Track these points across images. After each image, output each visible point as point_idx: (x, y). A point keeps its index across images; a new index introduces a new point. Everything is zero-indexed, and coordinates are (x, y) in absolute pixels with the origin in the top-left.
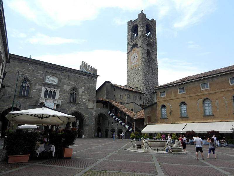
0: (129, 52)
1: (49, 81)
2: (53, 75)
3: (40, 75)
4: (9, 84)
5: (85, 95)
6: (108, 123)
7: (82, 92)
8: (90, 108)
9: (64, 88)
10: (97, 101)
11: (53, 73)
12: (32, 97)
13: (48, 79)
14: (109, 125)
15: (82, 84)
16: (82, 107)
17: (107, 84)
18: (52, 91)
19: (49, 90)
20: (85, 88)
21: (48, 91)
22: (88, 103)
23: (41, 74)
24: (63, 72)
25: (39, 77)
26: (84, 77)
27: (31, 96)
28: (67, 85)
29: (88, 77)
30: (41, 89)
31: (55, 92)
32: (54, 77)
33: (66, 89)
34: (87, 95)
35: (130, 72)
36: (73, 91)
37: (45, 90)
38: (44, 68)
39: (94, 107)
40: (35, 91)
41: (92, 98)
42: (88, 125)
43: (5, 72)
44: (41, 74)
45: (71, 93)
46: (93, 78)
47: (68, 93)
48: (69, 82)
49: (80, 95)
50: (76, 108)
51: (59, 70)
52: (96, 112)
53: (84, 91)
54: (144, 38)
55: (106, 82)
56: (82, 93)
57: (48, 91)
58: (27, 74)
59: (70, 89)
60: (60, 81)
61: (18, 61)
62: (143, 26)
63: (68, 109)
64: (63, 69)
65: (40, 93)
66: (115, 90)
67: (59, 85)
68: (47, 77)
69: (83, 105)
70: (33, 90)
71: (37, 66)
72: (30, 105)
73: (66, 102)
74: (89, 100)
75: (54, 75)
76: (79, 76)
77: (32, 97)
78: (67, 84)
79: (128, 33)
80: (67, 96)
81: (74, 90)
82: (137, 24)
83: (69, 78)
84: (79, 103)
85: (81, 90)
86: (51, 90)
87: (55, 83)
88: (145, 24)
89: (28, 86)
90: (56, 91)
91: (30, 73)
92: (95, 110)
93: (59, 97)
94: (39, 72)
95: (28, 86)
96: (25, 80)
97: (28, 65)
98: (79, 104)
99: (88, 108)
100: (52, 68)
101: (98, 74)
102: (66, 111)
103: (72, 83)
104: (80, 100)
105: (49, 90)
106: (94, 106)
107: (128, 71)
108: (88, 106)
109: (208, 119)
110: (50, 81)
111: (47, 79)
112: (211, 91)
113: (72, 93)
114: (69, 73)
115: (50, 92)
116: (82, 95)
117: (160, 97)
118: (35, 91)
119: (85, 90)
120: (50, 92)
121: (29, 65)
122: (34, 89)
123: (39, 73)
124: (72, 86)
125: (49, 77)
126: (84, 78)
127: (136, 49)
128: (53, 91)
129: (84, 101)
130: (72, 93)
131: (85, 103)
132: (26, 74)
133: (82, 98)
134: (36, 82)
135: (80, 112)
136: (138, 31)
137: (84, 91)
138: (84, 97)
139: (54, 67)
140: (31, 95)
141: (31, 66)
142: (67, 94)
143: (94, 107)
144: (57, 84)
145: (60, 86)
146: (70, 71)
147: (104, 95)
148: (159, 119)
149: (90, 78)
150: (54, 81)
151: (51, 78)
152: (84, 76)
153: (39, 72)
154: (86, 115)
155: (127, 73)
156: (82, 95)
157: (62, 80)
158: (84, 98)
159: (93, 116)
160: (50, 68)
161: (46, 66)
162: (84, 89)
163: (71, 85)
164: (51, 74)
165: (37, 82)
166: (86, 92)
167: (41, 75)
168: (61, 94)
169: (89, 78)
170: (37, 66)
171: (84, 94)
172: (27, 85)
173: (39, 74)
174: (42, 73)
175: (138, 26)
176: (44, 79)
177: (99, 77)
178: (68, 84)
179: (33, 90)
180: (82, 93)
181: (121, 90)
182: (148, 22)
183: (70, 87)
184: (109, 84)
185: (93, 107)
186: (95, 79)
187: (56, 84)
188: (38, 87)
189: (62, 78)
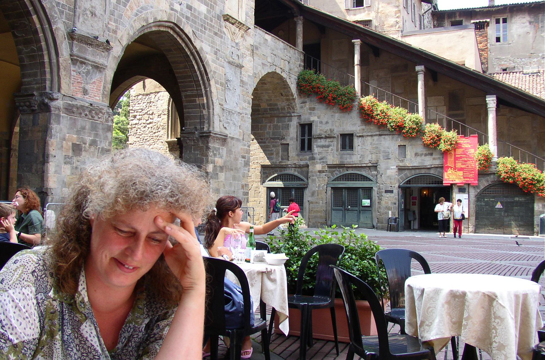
99: (227, 18)
106: (247, 14)
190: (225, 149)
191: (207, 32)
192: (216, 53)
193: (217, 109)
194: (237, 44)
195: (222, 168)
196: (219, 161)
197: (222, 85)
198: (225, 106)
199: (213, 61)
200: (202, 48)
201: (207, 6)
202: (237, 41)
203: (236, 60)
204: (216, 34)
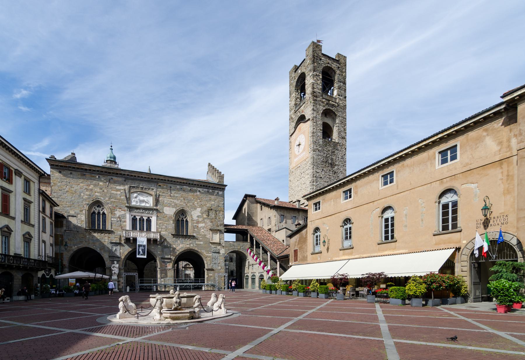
3: (119, 193)
5: (203, 221)
7: (198, 216)
14: (249, 269)
21: (138, 219)
23: (122, 191)
24: (160, 184)
28: (168, 207)
33: (168, 213)
36: (181, 217)
38: (125, 181)
39: (221, 240)
44: (122, 191)
45: (178, 220)
51: (153, 182)
52: (227, 249)
57: (138, 219)
64: (159, 179)
69: (201, 238)
71: (112, 177)
75: (146, 192)
78: (169, 205)
81: (183, 214)
83: (172, 195)
100: (139, 180)
104: (195, 229)
113: (180, 219)
125: (135, 195)
130: (180, 219)
133: (198, 226)
134: (115, 206)
138: (201, 225)
139: (142, 177)
143: (221, 240)
144: (152, 205)
146: (172, 181)
147: (245, 220)
156: (198, 222)
157: (160, 199)
160: (136, 179)
161: (128, 177)
164: (140, 191)
170: (112, 178)
171: (200, 220)
174: (122, 190)
180: (197, 218)
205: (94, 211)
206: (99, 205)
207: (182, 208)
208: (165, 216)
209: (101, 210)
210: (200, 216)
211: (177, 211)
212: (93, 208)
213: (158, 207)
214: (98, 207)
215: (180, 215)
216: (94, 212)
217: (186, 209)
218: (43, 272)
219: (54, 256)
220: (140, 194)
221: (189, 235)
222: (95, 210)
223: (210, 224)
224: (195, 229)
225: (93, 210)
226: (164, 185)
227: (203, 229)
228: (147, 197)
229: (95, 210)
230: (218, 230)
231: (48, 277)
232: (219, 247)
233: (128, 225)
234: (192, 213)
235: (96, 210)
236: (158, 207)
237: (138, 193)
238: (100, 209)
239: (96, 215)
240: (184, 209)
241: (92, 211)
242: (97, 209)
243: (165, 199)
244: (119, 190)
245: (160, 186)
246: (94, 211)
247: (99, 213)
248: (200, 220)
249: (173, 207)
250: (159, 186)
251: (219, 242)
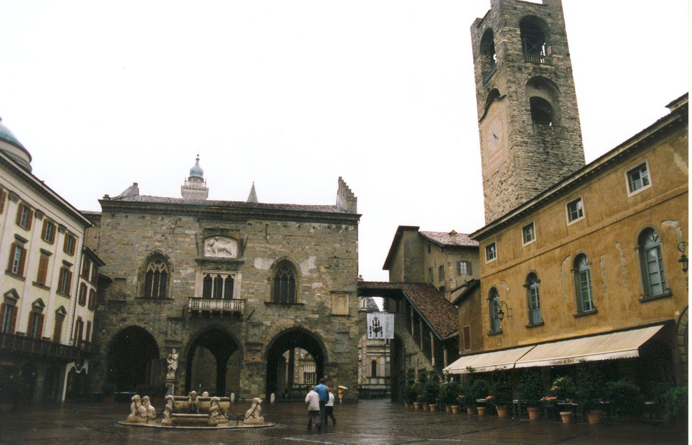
0: (481, 120)
1: (214, 251)
2: (224, 234)
3: (188, 240)
4: (121, 274)
5: (320, 279)
6: (403, 358)
7: (311, 271)
8: (338, 316)
9: (256, 266)
10: (361, 292)
11: (222, 230)
12: (174, 299)
13: (209, 248)
15: (307, 247)
16: (314, 312)
17: (406, 236)
18: (222, 279)
19: (213, 277)
20: (318, 257)
21: (213, 279)
22: (331, 299)
25: (186, 246)
26: (314, 228)
27: (170, 297)
29: (326, 225)
30: (193, 276)
31: (230, 281)
32: (227, 240)
34: (328, 278)
35: (490, 183)
37: (205, 275)
40: (179, 281)
41: (345, 285)
42: (335, 365)
43: (85, 248)
46: (344, 226)
47: (269, 279)
48: (269, 246)
49: (306, 279)
50: (293, 317)
53: (316, 267)
54: (516, 64)
55: (402, 230)
56: (309, 274)
57: (213, 279)
58: (159, 242)
59: (272, 267)
60: (242, 247)
61: (138, 215)
62: (506, 28)
63: (268, 323)
65: (192, 287)
66: (430, 252)
67: (240, 260)
68: (207, 242)
70: (175, 281)
71: (180, 217)
72: (170, 319)
73: (262, 303)
74: (332, 292)
76: (298, 225)
77: (173, 297)
79: (475, 58)
80: (265, 289)
82: (490, 25)
84: (304, 302)
85: (306, 267)
86: (219, 276)
87: (231, 254)
88: (515, 20)
89: (164, 272)
90: (234, 275)
91: (166, 239)
92: (356, 320)
93: (241, 292)
94: (187, 232)
95: (164, 272)
96: (157, 257)
97: (160, 218)
98: (302, 305)
101: (359, 212)
102: (264, 328)
103: (278, 248)
105: (213, 277)
106: (350, 309)
107: (486, 181)
108: (331, 310)
109: (583, 328)
110: (216, 250)
111: (207, 248)
112: (589, 226)
113: (281, 277)
114: (265, 222)
115: (219, 280)
116: (311, 280)
117: (486, 263)
118: (179, 281)
119: (319, 263)
120: (219, 280)
121: (162, 218)
122: (176, 279)
123: (187, 235)
124: (277, 258)
125: (212, 241)
126: (312, 231)
127: (495, 105)
128: (224, 277)
129: (320, 297)
130: (281, 277)
131: (323, 303)
132: (157, 244)
133: (310, 288)
135: (307, 327)
136: (495, 47)
137: (316, 267)
138: (315, 285)
140: (170, 294)
141: (167, 221)
142: (266, 281)
145: (243, 263)
148: (487, 336)
149: (334, 226)
150: (227, 251)
151: (219, 244)
152: (313, 224)
153: (187, 232)
154: (325, 337)
155: (484, 189)
156: (311, 280)
157: (249, 245)
158: (315, 289)
159: (350, 339)
162: (317, 260)
163: (274, 254)
165: (183, 260)
166: (323, 269)
167: (192, 239)
168: (247, 284)
169: (329, 228)
172: (161, 271)
173: (186, 237)
174: (192, 235)
175: (495, 31)
176: (200, 248)
177: (361, 218)
178: (264, 252)
179: (175, 281)
180: (309, 274)
181: (441, 251)
182: (530, 11)
183: (271, 262)
184: (415, 235)
185: (350, 312)
186: (351, 228)
187: (231, 257)
188: (183, 273)
189: (247, 239)
190: (337, 369)
191: (320, 324)
192: (327, 331)
193: (329, 353)
194: (343, 324)
195: (334, 377)
196: (332, 374)
197: (333, 343)
198: (336, 351)
199: (325, 335)
200: (316, 332)
201: (319, 314)
202: (343, 322)
203: (344, 331)
204: (326, 324)
205: (151, 269)
206: (158, 260)
207: (283, 259)
208: (257, 272)
209: (160, 267)
210: (314, 269)
211: (275, 263)
212: (150, 264)
213: (245, 259)
214: (156, 263)
215: (281, 269)
216: (151, 271)
217: (292, 259)
218: (72, 365)
219: (90, 340)
220: (219, 239)
221: (295, 302)
222: (152, 268)
223: (330, 282)
224: (306, 293)
225: (150, 267)
226: (257, 223)
227: (319, 291)
228: (229, 242)
229: (152, 268)
230: (346, 293)
231: (78, 372)
232: (348, 323)
233: (199, 291)
234: (301, 265)
235: (154, 267)
236: (245, 259)
237: (217, 237)
238: (160, 266)
239: (153, 276)
240: (287, 258)
241: (148, 269)
242: (156, 266)
243: (256, 245)
244: (187, 235)
245: (251, 224)
246: (151, 269)
247: (157, 271)
248: (314, 276)
249: (270, 257)
250: (249, 224)
251: (347, 314)
